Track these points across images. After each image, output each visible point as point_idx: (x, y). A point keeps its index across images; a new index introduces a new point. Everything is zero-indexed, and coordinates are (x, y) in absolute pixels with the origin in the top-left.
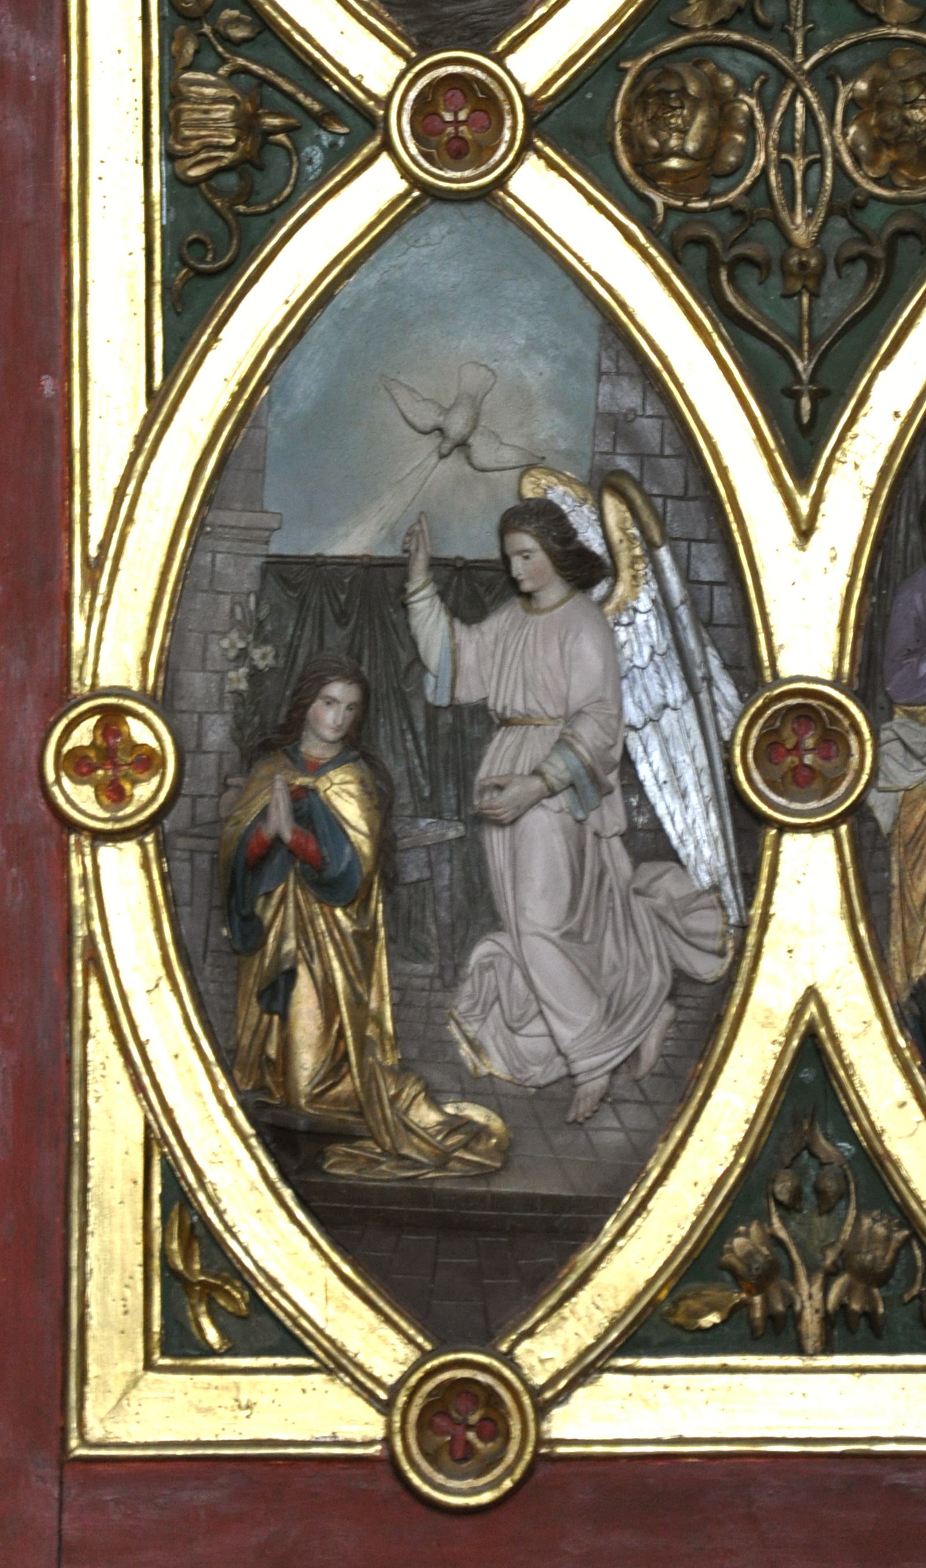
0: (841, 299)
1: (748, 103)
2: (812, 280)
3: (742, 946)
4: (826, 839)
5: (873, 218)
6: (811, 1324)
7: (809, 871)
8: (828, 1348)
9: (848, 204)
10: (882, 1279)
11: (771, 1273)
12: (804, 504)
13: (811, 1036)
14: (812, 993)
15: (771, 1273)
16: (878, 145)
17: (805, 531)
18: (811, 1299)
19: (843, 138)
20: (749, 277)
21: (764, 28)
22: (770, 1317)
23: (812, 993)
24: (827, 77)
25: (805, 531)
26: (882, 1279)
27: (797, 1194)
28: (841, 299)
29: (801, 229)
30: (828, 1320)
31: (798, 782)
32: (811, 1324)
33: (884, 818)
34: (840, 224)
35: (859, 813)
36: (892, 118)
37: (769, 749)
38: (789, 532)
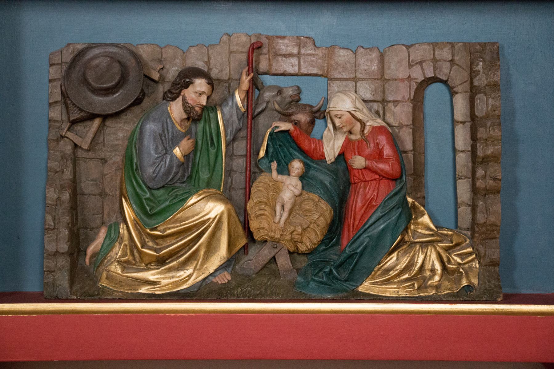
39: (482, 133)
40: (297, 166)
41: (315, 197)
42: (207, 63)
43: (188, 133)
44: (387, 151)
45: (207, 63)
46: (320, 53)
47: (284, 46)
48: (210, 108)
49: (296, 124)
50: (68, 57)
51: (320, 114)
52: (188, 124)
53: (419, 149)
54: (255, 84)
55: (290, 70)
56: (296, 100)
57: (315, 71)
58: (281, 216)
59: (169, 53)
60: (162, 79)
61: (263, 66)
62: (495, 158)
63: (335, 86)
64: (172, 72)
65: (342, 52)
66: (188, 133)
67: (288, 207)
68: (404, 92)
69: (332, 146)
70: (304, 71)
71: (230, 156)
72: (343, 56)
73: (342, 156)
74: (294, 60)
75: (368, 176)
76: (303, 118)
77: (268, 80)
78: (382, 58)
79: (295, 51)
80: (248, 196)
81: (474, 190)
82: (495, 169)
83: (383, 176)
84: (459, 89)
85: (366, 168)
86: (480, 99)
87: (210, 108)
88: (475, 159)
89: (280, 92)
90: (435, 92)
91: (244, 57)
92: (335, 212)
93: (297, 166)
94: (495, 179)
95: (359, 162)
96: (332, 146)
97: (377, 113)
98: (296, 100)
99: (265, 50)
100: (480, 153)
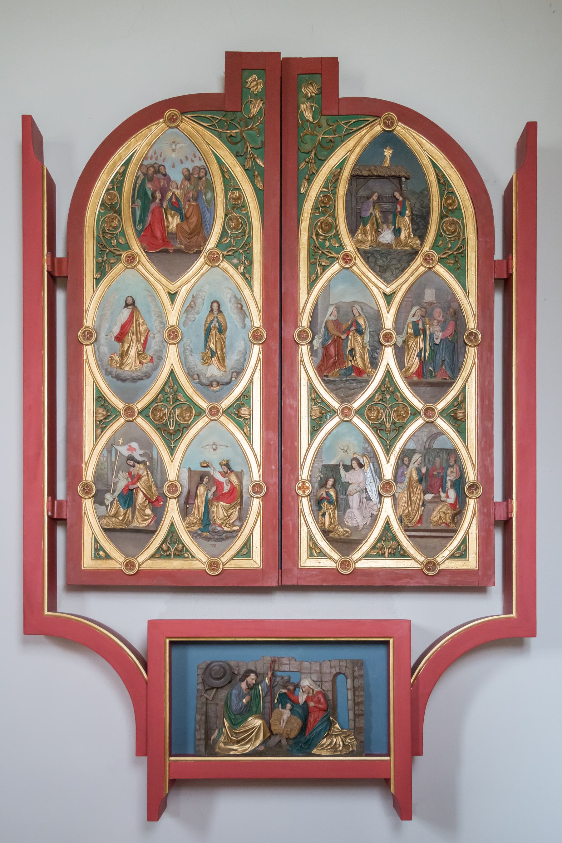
0: (393, 434)
1: (382, 410)
2: (389, 432)
3: (379, 510)
4: (390, 498)
5: (397, 425)
6: (386, 554)
7: (388, 502)
8: (388, 557)
9: (394, 423)
10: (395, 549)
11: (382, 548)
12: (388, 459)
13: (388, 521)
14: (388, 516)
15: (382, 548)
16: (397, 416)
17: (388, 462)
18: (387, 552)
19: (393, 415)
20: (382, 431)
21: (384, 401)
22: (382, 553)
23: (388, 516)
24: (391, 407)
25: (388, 462)
26: (395, 549)
27: (385, 540)
28: (393, 434)
29: (388, 426)
30: (389, 554)
31: (387, 491)
32: (386, 554)
33: (397, 496)
34: (393, 425)
35: (394, 495)
36: (399, 413)
37: (383, 488)
38: (386, 462)
39: (357, 693)
40: (289, 706)
41: (295, 717)
42: (256, 667)
43: (248, 694)
44: (322, 700)
45: (256, 667)
46: (297, 663)
47: (285, 661)
48: (257, 684)
49: (289, 690)
50: (204, 666)
51: (297, 686)
52: (248, 690)
53: (335, 699)
54: (273, 675)
55: (286, 670)
56: (288, 681)
57: (295, 670)
58: (283, 725)
59: (241, 664)
60: (239, 673)
61: (276, 668)
62: (362, 703)
63: (303, 676)
64: (242, 671)
65: (306, 663)
66: (248, 694)
67: (285, 721)
68: (328, 678)
69: (302, 699)
70: (291, 670)
71: (264, 702)
72: (306, 664)
73: (306, 702)
74: (288, 666)
75: (315, 709)
76: (291, 688)
77: (278, 673)
78: (320, 665)
79: (288, 663)
80: (270, 717)
81: (355, 715)
82: (362, 707)
83: (321, 710)
84: (349, 677)
85: (314, 706)
86: (356, 680)
87: (257, 684)
88: (356, 704)
89: (283, 678)
90: (340, 678)
91: (269, 665)
92: (303, 722)
93: (289, 706)
94: (362, 710)
95: (312, 704)
96: (302, 699)
97: (319, 686)
98: (288, 681)
99: (277, 662)
100: (356, 701)
